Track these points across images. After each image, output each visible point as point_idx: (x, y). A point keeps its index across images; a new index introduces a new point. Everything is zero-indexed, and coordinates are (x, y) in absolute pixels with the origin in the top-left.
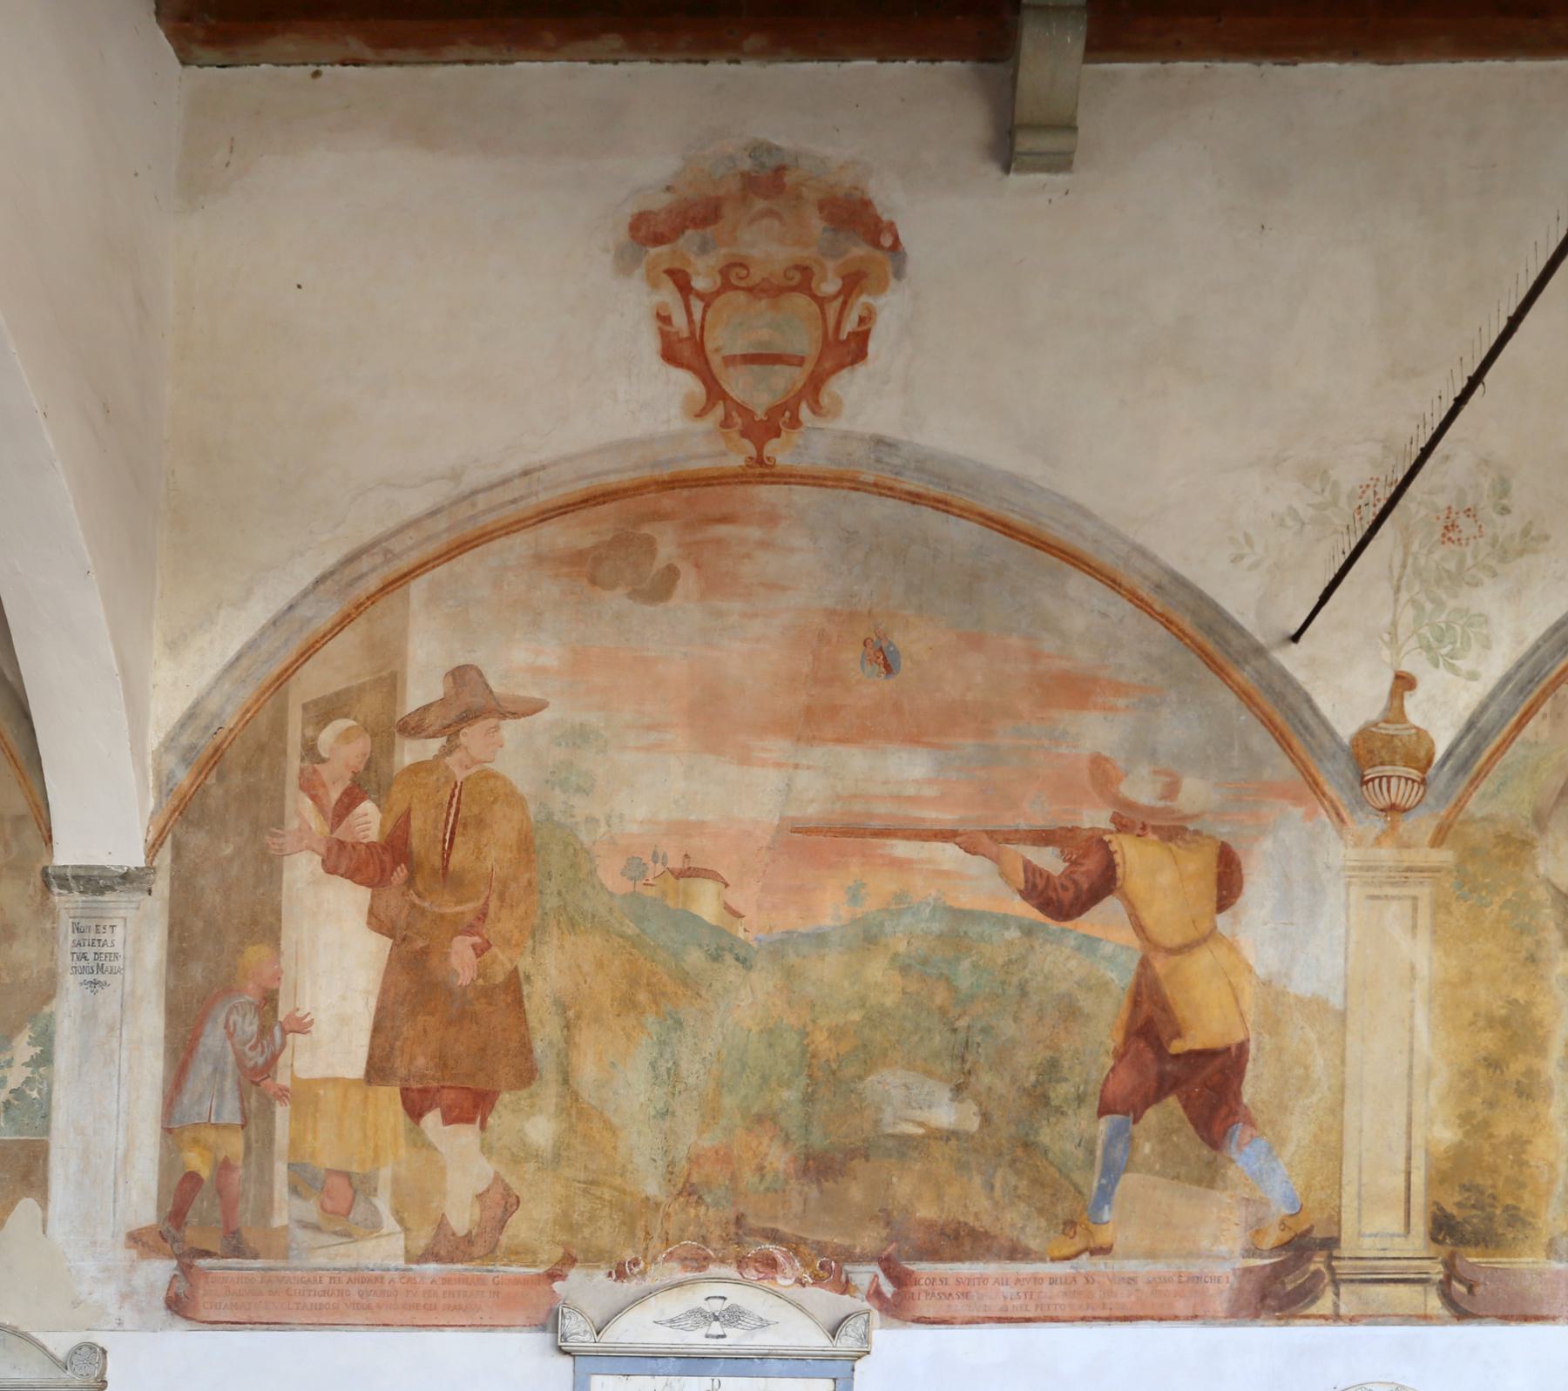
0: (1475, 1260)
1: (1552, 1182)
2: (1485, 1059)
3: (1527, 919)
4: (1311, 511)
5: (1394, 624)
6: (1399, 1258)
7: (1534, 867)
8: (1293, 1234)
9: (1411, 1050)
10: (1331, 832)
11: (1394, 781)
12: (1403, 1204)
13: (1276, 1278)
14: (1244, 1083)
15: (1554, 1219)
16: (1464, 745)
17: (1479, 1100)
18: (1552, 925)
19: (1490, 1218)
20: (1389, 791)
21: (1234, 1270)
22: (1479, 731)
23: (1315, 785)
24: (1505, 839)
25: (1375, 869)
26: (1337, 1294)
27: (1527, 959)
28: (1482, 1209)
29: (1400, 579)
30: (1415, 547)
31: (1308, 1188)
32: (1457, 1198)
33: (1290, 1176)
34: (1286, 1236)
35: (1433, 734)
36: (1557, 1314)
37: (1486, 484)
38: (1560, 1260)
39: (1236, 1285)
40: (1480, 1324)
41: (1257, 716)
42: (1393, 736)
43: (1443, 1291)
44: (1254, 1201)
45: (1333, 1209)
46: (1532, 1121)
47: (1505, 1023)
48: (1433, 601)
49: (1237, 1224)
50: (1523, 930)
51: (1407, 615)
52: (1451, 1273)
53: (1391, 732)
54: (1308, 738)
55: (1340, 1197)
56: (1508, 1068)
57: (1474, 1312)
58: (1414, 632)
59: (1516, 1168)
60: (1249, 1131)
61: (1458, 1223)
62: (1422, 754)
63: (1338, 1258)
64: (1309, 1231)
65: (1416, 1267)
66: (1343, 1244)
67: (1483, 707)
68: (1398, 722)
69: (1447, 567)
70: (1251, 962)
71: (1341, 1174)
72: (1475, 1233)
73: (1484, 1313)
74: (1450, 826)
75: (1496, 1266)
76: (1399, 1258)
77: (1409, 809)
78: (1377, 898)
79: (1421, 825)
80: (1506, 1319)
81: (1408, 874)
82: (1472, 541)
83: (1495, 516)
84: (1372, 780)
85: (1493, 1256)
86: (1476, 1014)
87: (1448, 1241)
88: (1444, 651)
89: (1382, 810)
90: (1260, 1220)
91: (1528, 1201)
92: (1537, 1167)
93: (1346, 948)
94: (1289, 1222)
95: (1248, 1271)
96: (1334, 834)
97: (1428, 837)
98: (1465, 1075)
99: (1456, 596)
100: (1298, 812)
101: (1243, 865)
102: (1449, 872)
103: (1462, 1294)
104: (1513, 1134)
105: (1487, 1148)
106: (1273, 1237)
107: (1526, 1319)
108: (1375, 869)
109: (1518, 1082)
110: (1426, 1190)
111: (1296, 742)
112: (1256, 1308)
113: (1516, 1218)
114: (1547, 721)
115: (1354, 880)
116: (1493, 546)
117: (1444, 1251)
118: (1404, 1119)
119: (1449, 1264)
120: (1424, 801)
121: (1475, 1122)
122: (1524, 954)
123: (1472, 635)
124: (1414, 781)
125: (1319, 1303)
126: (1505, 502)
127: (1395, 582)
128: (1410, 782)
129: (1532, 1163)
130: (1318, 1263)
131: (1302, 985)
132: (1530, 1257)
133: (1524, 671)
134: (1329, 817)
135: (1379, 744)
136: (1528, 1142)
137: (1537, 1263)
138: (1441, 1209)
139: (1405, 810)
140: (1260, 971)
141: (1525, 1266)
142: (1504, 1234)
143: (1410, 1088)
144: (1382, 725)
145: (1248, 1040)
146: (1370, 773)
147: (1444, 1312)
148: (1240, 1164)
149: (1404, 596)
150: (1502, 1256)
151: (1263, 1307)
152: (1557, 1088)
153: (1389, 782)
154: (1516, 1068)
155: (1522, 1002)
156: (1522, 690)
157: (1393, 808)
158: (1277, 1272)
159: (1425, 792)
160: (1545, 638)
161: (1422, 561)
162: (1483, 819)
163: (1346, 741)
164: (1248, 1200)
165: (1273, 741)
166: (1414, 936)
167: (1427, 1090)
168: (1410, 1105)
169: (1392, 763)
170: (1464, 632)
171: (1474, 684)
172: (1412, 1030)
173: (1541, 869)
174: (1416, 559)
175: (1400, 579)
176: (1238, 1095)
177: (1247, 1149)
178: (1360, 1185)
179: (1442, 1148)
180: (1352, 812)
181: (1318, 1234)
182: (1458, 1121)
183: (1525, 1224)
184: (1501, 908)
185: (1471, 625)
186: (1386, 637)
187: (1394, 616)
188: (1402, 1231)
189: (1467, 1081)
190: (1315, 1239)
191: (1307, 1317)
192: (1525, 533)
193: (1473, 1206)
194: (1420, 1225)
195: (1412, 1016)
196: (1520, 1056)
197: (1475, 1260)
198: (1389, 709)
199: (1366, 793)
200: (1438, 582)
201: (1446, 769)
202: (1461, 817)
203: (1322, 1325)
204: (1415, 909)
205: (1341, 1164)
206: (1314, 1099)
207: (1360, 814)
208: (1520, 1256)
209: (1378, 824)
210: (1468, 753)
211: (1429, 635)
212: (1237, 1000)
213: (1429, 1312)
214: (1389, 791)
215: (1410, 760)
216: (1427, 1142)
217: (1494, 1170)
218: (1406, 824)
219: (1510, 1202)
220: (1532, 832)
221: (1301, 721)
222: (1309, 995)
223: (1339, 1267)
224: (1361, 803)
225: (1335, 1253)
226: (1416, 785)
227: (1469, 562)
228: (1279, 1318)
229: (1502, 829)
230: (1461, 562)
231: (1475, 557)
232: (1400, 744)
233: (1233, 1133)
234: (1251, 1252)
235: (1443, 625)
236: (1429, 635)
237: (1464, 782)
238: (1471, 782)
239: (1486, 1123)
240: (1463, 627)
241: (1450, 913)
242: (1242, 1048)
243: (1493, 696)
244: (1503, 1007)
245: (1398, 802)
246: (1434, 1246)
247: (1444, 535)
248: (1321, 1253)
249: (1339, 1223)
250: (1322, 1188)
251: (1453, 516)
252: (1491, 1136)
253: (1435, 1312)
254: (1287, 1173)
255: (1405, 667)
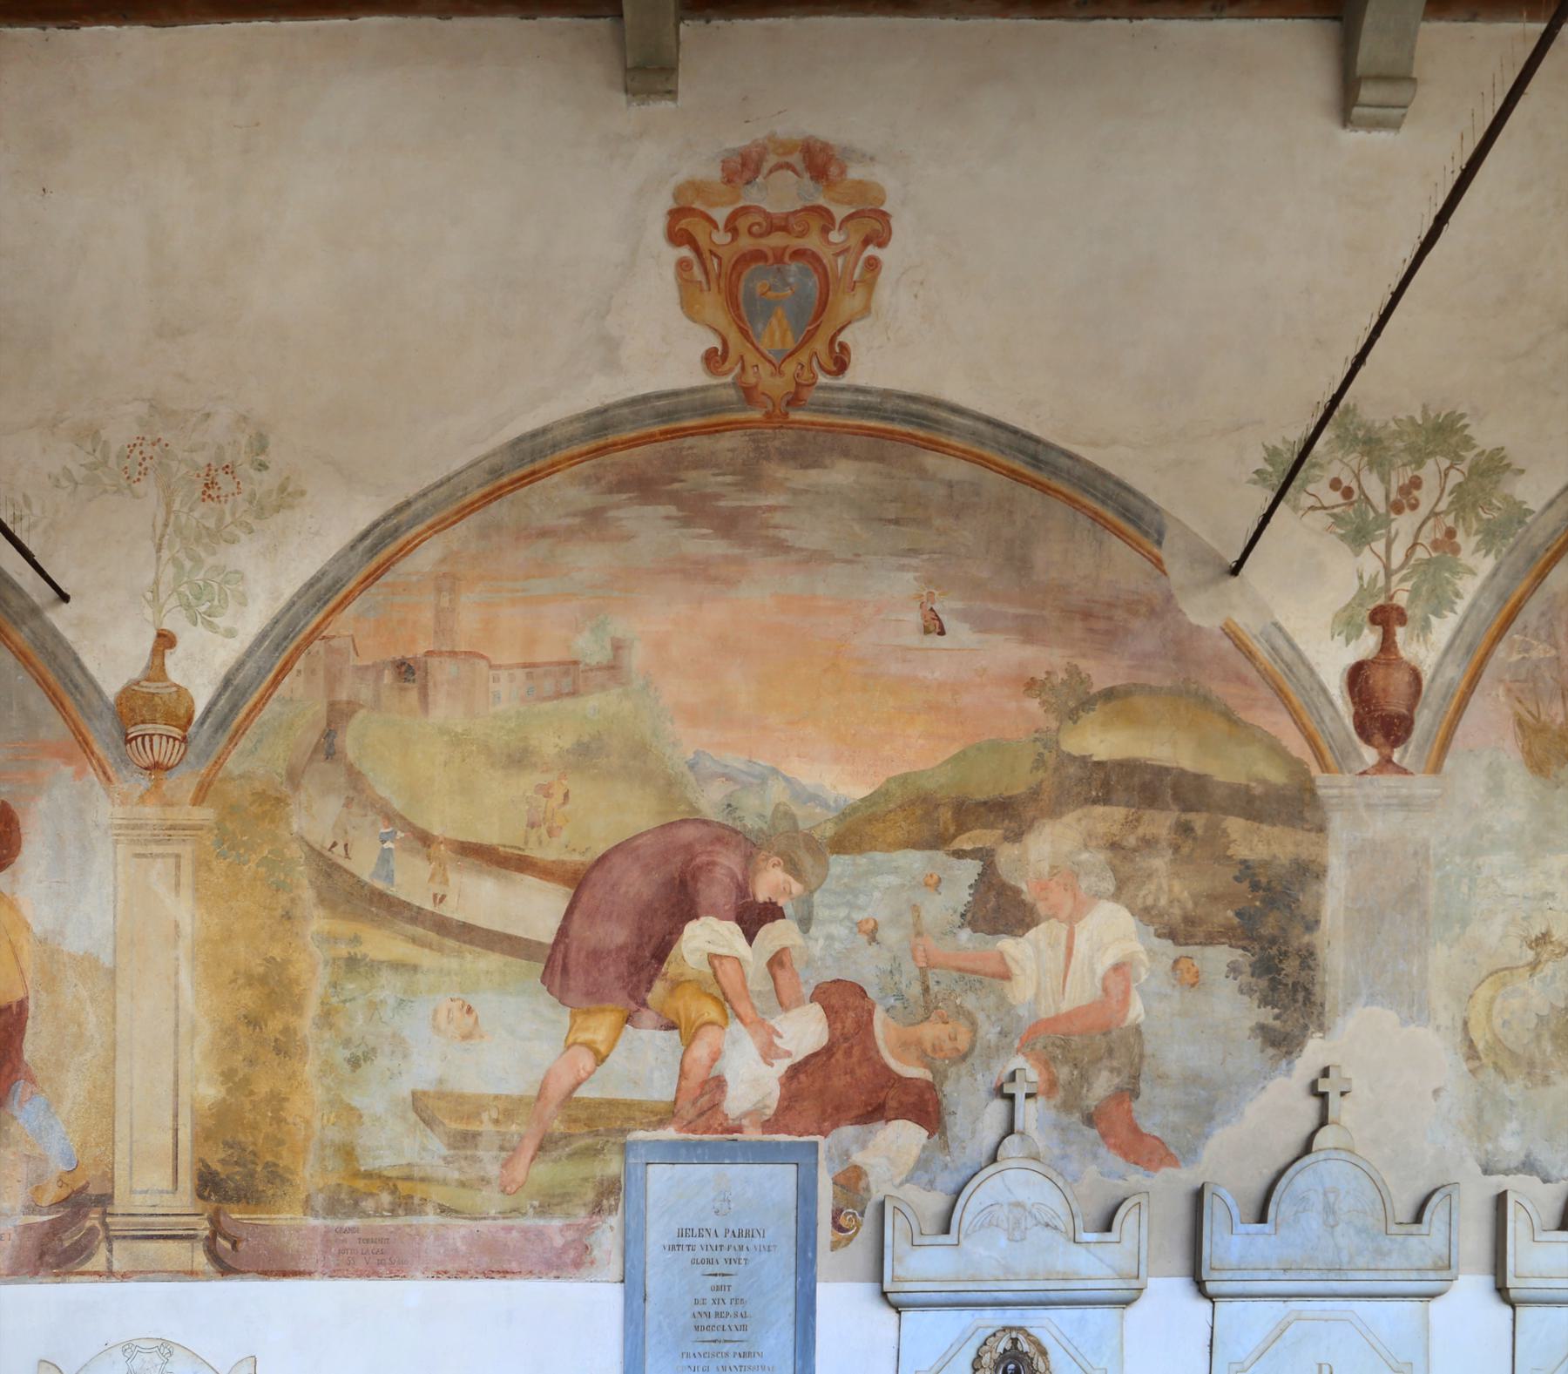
0: (238, 1216)
1: (307, 1139)
2: (245, 1017)
3: (282, 877)
4: (84, 471)
5: (156, 582)
6: (168, 1215)
7: (289, 824)
8: (70, 1191)
9: (177, 1008)
10: (99, 789)
11: (156, 739)
12: (171, 1160)
13: (55, 1235)
14: (25, 1041)
15: (312, 1176)
16: (222, 702)
17: (241, 1058)
18: (305, 882)
19: (252, 1174)
20: (152, 749)
21: (15, 1227)
22: (236, 689)
23: (84, 744)
24: (261, 797)
25: (140, 827)
26: (110, 1251)
27: (283, 916)
28: (245, 1166)
29: (162, 536)
30: (176, 506)
31: (84, 1144)
32: (221, 1155)
33: (67, 1133)
34: (64, 1193)
35: (192, 691)
36: (313, 1270)
37: (244, 440)
38: (316, 1216)
39: (17, 1242)
40: (242, 1279)
41: (32, 675)
42: (153, 694)
43: (208, 1247)
44: (35, 1158)
45: (107, 1166)
46: (290, 1079)
47: (263, 980)
48: (192, 559)
49: (19, 1181)
50: (279, 888)
51: (169, 572)
52: (217, 1230)
53: (152, 690)
54: (78, 697)
55: (113, 1154)
56: (266, 1025)
57: (237, 1267)
58: (174, 590)
59: (275, 1126)
60: (30, 1088)
61: (222, 1180)
62: (182, 712)
63: (112, 1215)
64: (85, 1188)
65: (184, 1224)
66: (116, 1202)
67: (240, 665)
68: (159, 681)
69: (207, 525)
70: (29, 920)
71: (113, 1131)
72: (237, 1189)
73: (246, 1269)
74: (210, 785)
75: (257, 1222)
76: (168, 1215)
77: (172, 767)
78: (143, 856)
79: (183, 782)
80: (266, 1274)
81: (171, 832)
82: (230, 498)
83: (252, 472)
84: (135, 738)
85: (255, 1213)
86: (235, 973)
87: (213, 1198)
88: (203, 609)
89: (146, 769)
90: (40, 1177)
91: (286, 1159)
92: (295, 1124)
93: (115, 907)
94: (67, 1179)
95: (28, 1227)
96: (102, 792)
97: (191, 795)
98: (228, 1031)
99: (214, 553)
100: (68, 771)
101: (21, 824)
102: (211, 830)
103: (226, 1250)
104: (272, 1091)
105: (248, 1106)
106: (52, 1193)
107: (284, 1274)
108: (140, 827)
109: (276, 1040)
110: (193, 1146)
111: (68, 701)
112: (35, 1266)
113: (276, 1175)
114: (302, 678)
115: (122, 838)
116: (251, 503)
117: (210, 1207)
118: (170, 1077)
119: (214, 1221)
120: (184, 760)
121: (237, 1079)
122: (280, 912)
123: (228, 592)
124: (175, 739)
125: (94, 1260)
126: (262, 458)
127: (157, 541)
128: (171, 740)
129: (290, 1120)
130: (93, 1220)
131: (74, 944)
132: (288, 1212)
133: (280, 627)
134: (97, 775)
135: (140, 702)
136: (286, 1099)
137: (295, 1219)
138: (207, 1166)
139: (168, 769)
140: (37, 929)
141: (284, 1223)
142: (264, 1191)
143: (176, 1044)
144: (144, 683)
145: (28, 998)
146: (134, 731)
147: (210, 1268)
148: (21, 1121)
149: (165, 554)
150: (262, 1213)
151: (42, 1265)
152: (311, 1046)
153: (151, 741)
154: (274, 1026)
155: (279, 960)
156: (278, 647)
157: (156, 766)
158: (55, 1229)
159: (186, 749)
160: (299, 595)
161: (183, 519)
162: (241, 776)
163: (112, 699)
164: (29, 1156)
165: (47, 699)
166: (178, 893)
167: (192, 1048)
168: (176, 1062)
169: (154, 721)
170: (221, 588)
171: (231, 641)
172: (176, 988)
173: (295, 827)
174: (177, 517)
175: (162, 536)
176: (19, 1051)
177: (27, 1106)
178: (131, 1143)
179: (206, 1106)
180: (118, 771)
181: (93, 1190)
182: (221, 1079)
183: (284, 1181)
184: (258, 865)
185: (227, 582)
186: (149, 595)
187: (157, 574)
188: (170, 1188)
189: (228, 1038)
190: (90, 1196)
191: (82, 1274)
192: (283, 489)
193: (236, 1163)
194: (187, 1182)
195: (177, 973)
196: (277, 1014)
197: (238, 1216)
198: (149, 667)
199: (129, 751)
200: (198, 539)
201: (205, 727)
202: (220, 775)
203: (96, 1282)
204: (178, 867)
205: (114, 1121)
206: (88, 1055)
207: (125, 772)
208: (279, 1212)
209: (144, 782)
210: (226, 710)
211: (188, 593)
212: (16, 957)
213: (196, 1267)
214: (152, 749)
215: (170, 718)
216: (193, 1099)
217: (254, 1127)
218: (170, 782)
219: (269, 1158)
220: (286, 790)
221: (71, 681)
222: (81, 953)
223: (113, 1224)
224: (125, 761)
225: (109, 1210)
226: (177, 742)
227: (228, 519)
228: (57, 1275)
229: (258, 786)
230: (220, 519)
231: (233, 514)
232: (160, 702)
233: (16, 1091)
234: (31, 1209)
235: (201, 583)
236: (188, 593)
237: (224, 739)
238: (231, 739)
239: (246, 1081)
240: (219, 584)
241: (210, 870)
242: (22, 1005)
243: (249, 653)
244: (261, 965)
245: (161, 761)
246: (201, 1203)
247: (204, 493)
248: (96, 1209)
249: (112, 1180)
250: (97, 1145)
251: (212, 473)
252: (252, 1093)
253: (201, 1268)
254: (64, 1129)
255: (167, 625)
